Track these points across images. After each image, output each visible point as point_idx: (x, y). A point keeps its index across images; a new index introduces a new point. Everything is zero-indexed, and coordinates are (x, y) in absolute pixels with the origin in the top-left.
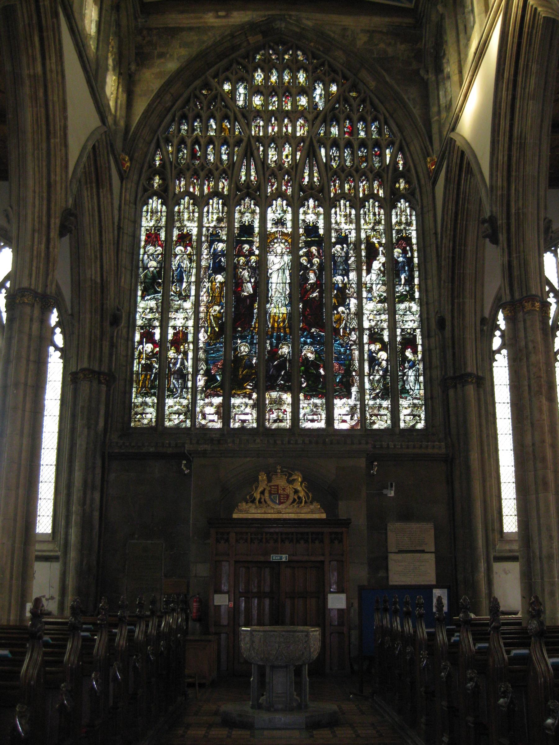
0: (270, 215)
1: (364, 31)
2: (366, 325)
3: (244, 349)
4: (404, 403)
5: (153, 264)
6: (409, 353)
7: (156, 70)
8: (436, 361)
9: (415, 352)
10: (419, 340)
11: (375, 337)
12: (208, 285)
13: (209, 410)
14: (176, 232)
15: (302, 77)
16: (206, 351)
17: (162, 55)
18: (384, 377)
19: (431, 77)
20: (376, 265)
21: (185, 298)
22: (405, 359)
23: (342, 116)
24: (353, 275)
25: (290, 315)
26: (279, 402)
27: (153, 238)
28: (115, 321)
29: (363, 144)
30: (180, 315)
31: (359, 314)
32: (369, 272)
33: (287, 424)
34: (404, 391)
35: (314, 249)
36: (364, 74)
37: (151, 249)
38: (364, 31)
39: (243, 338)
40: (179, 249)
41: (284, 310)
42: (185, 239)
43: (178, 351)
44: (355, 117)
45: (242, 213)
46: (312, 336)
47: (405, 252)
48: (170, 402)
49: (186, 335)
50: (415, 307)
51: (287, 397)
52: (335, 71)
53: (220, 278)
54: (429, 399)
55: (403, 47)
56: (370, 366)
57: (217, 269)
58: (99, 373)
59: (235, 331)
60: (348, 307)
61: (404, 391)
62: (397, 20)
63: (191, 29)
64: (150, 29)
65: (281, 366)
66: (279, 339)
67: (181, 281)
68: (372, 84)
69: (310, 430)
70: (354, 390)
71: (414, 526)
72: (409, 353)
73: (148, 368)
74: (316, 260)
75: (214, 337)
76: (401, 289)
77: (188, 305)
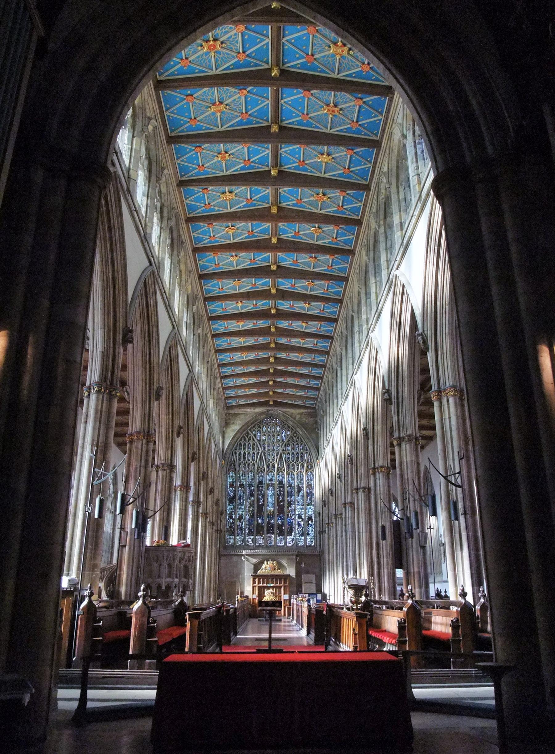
0: (268, 478)
1: (298, 414)
2: (297, 513)
3: (260, 521)
4: (308, 537)
5: (232, 494)
6: (310, 522)
7: (231, 429)
8: (318, 525)
9: (312, 522)
10: (313, 518)
11: (300, 517)
12: (249, 501)
13: (249, 540)
14: (239, 483)
15: (278, 429)
16: (249, 522)
17: (233, 423)
18: (302, 530)
19: (319, 432)
20: (301, 494)
21: (242, 505)
22: (309, 524)
23: (291, 444)
24: (293, 497)
25: (274, 510)
26: (271, 537)
27: (232, 485)
28: (222, 514)
29: (298, 453)
30: (241, 510)
31: (295, 510)
32: (298, 496)
33: (273, 544)
34: (308, 534)
35: (281, 489)
36: (298, 429)
37: (231, 489)
38: (298, 414)
39: (260, 518)
40: (240, 489)
41: (272, 509)
42: (242, 486)
43: (240, 522)
44: (295, 444)
45: (259, 477)
46: (280, 517)
47: (310, 489)
48: (238, 537)
49: (242, 517)
50: (312, 507)
51: (273, 536)
52: (289, 427)
53: (252, 498)
54: (315, 536)
55: (311, 419)
56: (298, 526)
57: (252, 495)
58: (218, 530)
59: (257, 515)
60: (291, 507)
61: (308, 534)
62: (309, 411)
63: (242, 414)
64: (229, 414)
65: (271, 526)
66: (271, 518)
67: (240, 499)
68: (301, 433)
69: (280, 546)
70: (293, 533)
71: (310, 575)
72: (310, 522)
73: (231, 527)
74: (282, 493)
75: (252, 517)
76: (308, 502)
77: (243, 507)
